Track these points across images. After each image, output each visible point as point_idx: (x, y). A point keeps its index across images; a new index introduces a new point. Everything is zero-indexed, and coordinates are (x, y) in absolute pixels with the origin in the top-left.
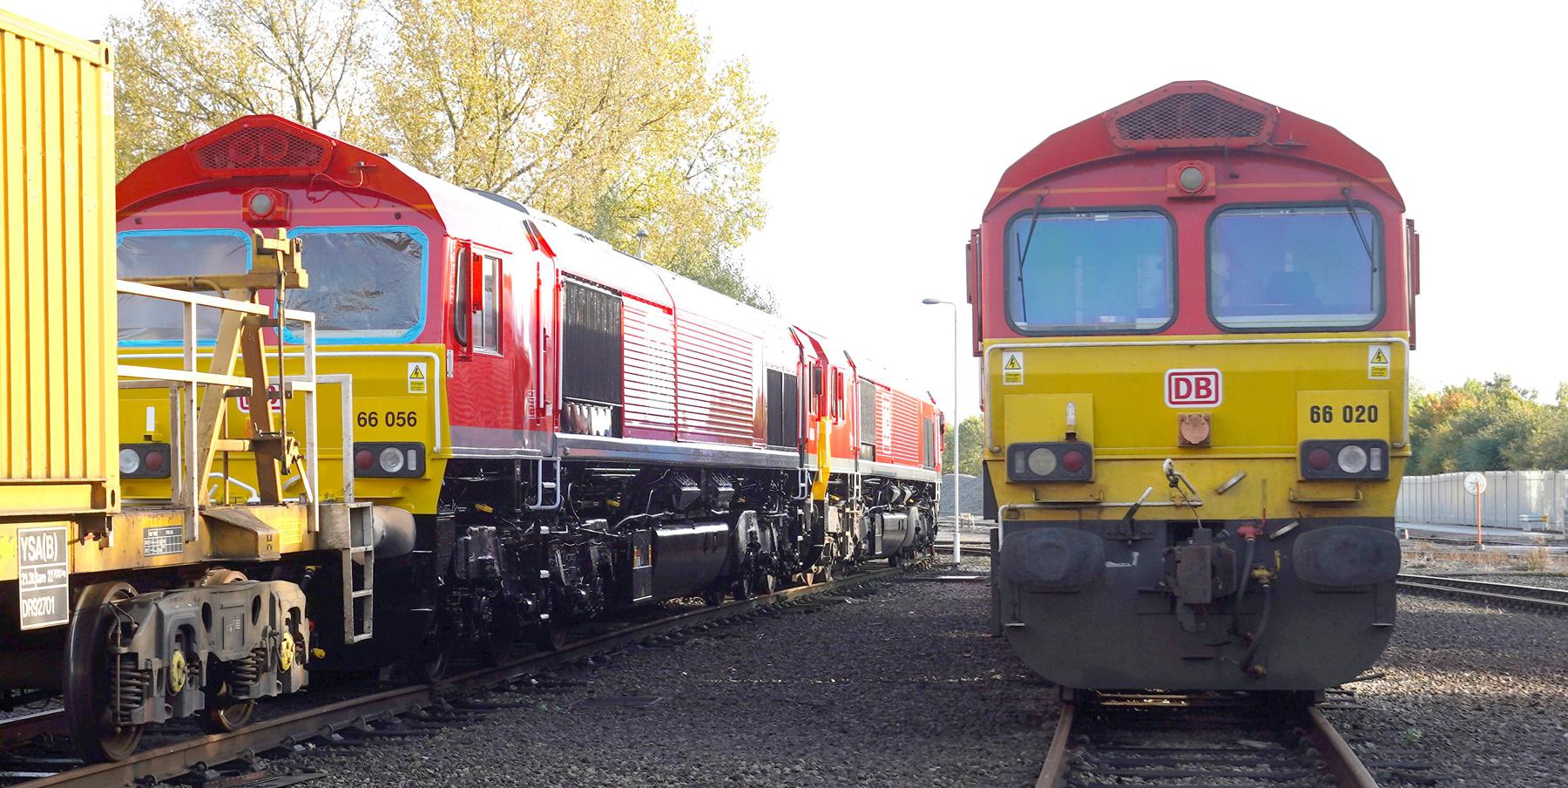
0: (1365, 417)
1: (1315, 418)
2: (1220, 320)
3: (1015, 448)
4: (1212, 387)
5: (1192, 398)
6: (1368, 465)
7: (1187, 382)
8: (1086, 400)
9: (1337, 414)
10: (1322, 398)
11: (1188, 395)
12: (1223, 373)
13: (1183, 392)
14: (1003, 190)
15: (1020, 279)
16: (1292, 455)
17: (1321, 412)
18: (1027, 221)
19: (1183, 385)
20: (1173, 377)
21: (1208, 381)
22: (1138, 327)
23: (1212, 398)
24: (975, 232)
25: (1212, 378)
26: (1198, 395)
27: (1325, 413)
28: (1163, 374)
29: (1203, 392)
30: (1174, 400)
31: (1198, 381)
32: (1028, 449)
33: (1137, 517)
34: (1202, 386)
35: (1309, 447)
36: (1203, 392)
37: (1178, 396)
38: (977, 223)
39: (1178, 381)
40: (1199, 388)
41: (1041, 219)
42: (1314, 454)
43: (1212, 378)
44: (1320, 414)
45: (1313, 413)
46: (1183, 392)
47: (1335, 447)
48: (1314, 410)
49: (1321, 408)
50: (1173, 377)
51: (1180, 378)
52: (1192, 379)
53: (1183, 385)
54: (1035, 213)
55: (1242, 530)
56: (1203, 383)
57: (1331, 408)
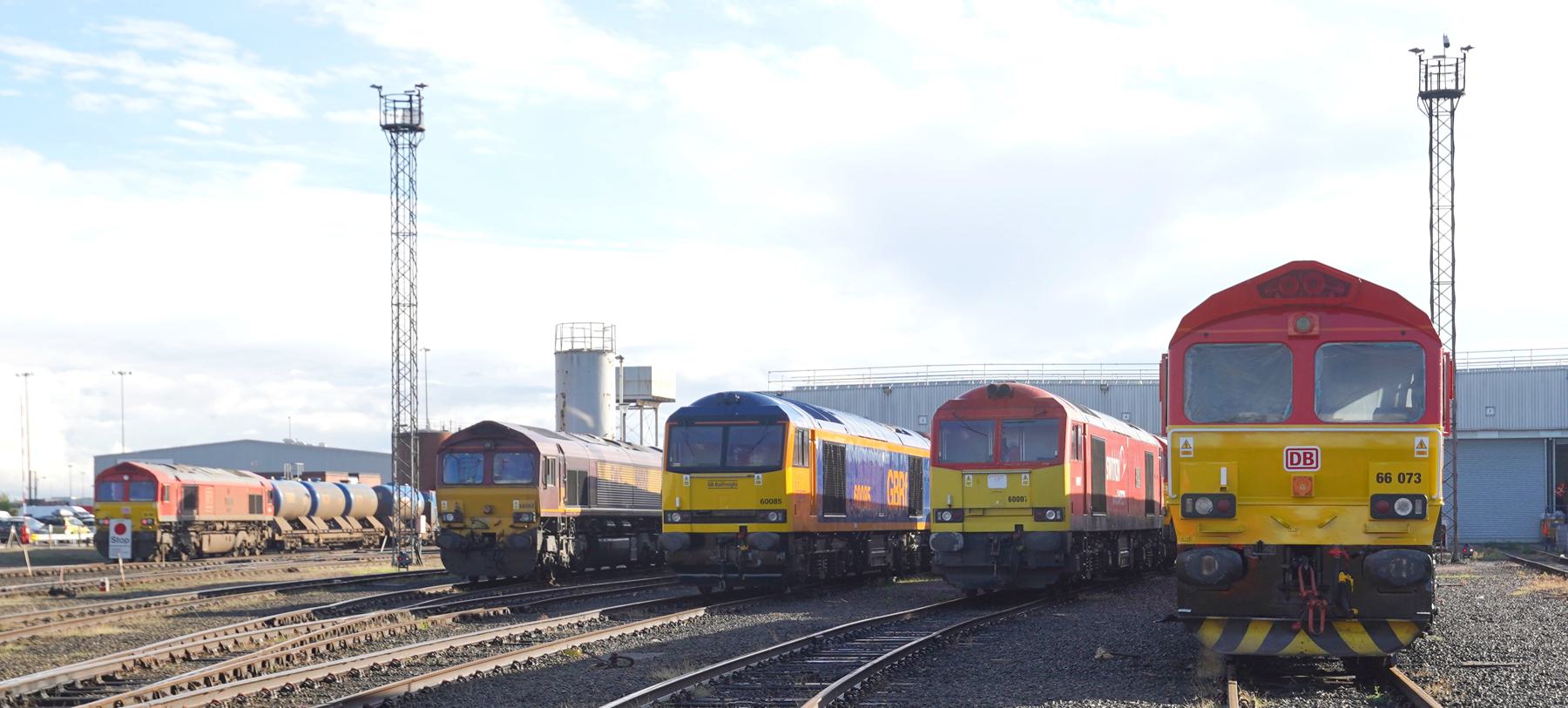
0: (1407, 477)
3: (1185, 496)
4: (1314, 458)
5: (1301, 465)
6: (1413, 510)
9: (1395, 478)
11: (1298, 463)
14: (1184, 330)
19: (1295, 457)
20: (1289, 452)
23: (1314, 465)
24: (1164, 356)
25: (1314, 452)
26: (1305, 464)
28: (1283, 450)
29: (1308, 461)
30: (1289, 466)
31: (1305, 454)
32: (1195, 497)
34: (1307, 457)
35: (1375, 499)
36: (1308, 461)
37: (1292, 464)
38: (1166, 351)
39: (1292, 454)
40: (1305, 458)
42: (1383, 504)
43: (1314, 452)
44: (1383, 478)
47: (1393, 498)
50: (1289, 452)
51: (1292, 453)
52: (1301, 452)
53: (1295, 457)
55: (1332, 552)
56: (1308, 456)
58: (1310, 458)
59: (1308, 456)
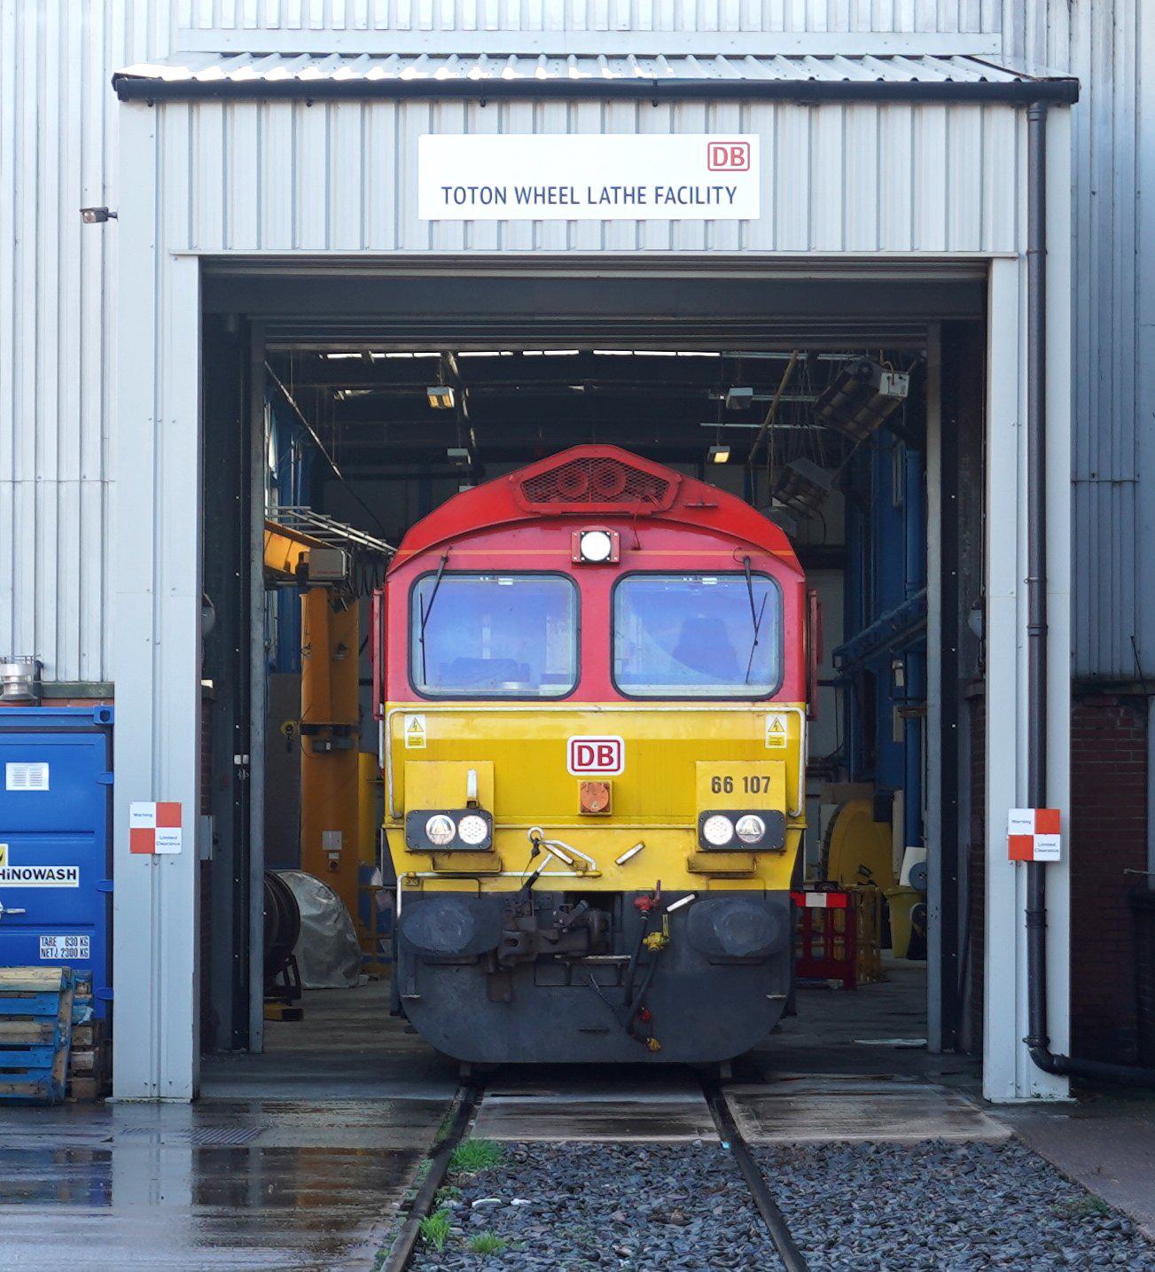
1: (716, 789)
2: (622, 687)
4: (614, 755)
5: (595, 765)
8: (487, 767)
9: (739, 785)
10: (722, 769)
11: (591, 761)
12: (625, 741)
13: (586, 759)
15: (422, 641)
16: (692, 826)
17: (722, 783)
18: (432, 581)
20: (576, 745)
21: (610, 750)
22: (541, 694)
23: (614, 766)
25: (614, 746)
26: (600, 763)
27: (726, 783)
28: (566, 741)
29: (605, 760)
30: (577, 767)
31: (600, 748)
33: (537, 886)
34: (604, 754)
36: (605, 760)
37: (580, 763)
40: (601, 755)
41: (446, 579)
43: (614, 746)
45: (714, 783)
46: (586, 759)
48: (715, 780)
49: (722, 779)
50: (576, 745)
52: (595, 746)
54: (439, 575)
55: (638, 902)
56: (605, 751)
57: (731, 779)
58: (605, 755)
59: (605, 751)
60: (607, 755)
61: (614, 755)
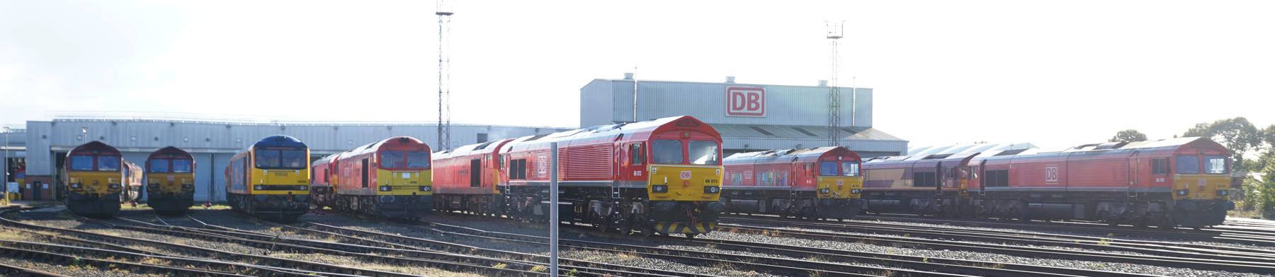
4: (760, 101)
5: (745, 110)
7: (742, 95)
11: (742, 108)
13: (739, 105)
19: (739, 98)
20: (732, 92)
23: (759, 111)
26: (749, 108)
30: (731, 111)
31: (749, 95)
37: (735, 108)
39: (735, 95)
40: (750, 101)
46: (739, 105)
52: (745, 93)
53: (739, 98)
58: (755, 101)
59: (753, 98)
60: (755, 101)
61: (760, 101)
